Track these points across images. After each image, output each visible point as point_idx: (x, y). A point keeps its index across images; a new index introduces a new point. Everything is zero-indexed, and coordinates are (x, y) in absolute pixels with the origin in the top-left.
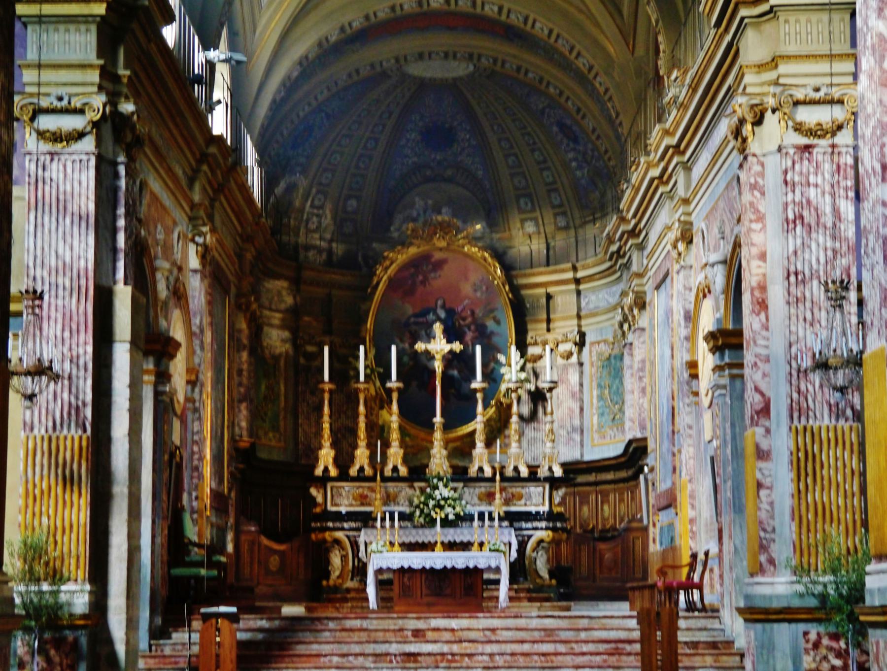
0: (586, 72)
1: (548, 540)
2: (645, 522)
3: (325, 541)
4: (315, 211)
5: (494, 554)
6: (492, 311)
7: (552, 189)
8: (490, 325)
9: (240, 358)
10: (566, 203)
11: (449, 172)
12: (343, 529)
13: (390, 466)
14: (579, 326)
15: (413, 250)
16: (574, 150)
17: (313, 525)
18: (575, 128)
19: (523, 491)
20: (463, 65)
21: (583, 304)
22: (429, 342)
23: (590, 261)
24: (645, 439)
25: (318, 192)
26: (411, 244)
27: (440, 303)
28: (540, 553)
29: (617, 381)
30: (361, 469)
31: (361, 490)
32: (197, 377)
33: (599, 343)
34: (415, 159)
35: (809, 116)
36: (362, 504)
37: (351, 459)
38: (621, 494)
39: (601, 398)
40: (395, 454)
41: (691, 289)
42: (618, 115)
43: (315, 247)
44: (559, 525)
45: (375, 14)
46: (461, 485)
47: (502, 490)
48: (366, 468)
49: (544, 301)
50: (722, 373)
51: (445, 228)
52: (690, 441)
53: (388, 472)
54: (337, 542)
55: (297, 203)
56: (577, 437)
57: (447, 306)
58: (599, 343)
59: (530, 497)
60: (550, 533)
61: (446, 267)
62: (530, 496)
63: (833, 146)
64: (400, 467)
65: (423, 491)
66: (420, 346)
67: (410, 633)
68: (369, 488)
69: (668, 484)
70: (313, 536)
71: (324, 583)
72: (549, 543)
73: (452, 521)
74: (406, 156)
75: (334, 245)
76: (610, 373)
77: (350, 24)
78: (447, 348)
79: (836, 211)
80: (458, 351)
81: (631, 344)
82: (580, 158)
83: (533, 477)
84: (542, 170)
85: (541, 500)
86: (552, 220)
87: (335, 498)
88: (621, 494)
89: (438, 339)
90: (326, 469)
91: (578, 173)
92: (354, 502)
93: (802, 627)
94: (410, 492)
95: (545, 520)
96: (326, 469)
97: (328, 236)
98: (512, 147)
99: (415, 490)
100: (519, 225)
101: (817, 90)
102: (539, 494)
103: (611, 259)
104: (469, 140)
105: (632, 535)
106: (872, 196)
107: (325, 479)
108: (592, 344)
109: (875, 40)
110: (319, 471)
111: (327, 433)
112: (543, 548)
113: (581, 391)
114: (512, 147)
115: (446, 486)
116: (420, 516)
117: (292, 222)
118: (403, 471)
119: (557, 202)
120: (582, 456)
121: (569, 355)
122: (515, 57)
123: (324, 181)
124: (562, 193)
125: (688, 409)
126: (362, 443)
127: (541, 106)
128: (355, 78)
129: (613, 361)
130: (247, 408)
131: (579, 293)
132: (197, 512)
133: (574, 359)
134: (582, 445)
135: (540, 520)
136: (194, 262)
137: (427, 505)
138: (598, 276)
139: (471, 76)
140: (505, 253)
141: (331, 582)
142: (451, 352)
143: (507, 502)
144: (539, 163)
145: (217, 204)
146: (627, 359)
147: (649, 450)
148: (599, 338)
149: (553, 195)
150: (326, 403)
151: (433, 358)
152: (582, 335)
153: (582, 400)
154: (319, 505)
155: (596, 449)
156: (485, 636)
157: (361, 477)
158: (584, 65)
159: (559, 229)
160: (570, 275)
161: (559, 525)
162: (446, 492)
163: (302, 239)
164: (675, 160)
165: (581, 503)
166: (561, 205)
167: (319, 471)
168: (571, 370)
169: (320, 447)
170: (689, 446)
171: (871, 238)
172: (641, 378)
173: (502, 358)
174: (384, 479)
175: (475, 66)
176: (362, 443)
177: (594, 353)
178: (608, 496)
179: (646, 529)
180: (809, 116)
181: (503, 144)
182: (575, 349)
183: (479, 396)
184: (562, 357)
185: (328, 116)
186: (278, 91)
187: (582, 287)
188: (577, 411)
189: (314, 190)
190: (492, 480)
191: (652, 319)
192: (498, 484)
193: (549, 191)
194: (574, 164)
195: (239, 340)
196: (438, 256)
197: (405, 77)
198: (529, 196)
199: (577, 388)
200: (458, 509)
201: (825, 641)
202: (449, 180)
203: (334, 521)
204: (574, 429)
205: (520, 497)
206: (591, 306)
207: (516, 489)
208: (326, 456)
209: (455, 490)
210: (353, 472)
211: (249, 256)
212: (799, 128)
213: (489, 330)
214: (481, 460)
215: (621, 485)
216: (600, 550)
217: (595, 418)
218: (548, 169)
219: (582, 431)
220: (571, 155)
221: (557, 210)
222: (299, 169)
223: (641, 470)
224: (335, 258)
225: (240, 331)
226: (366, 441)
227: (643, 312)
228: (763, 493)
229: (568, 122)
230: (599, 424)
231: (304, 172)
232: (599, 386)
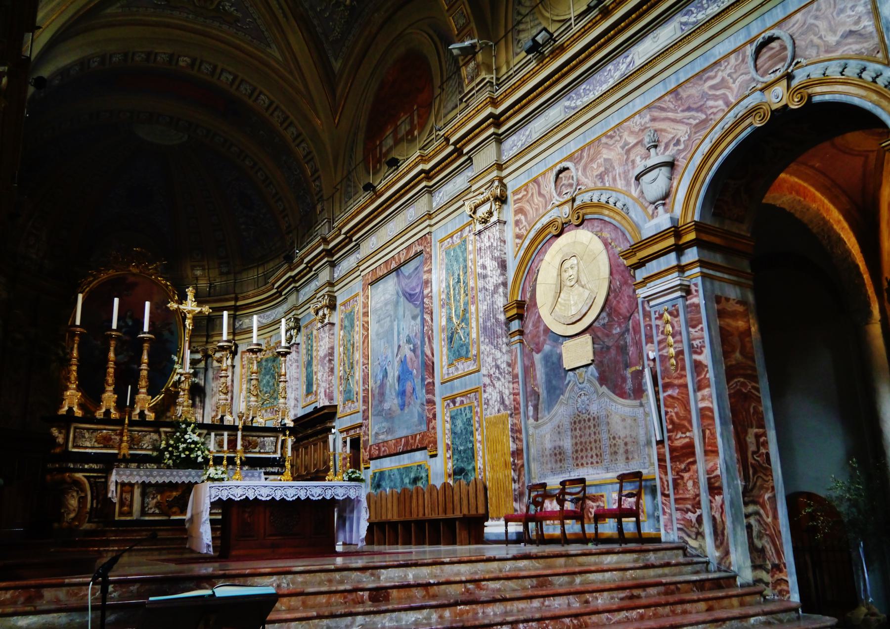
5: (353, 483)
8: (166, 334)
12: (83, 470)
13: (138, 411)
17: (49, 466)
19: (259, 440)
21: (237, 325)
29: (268, 377)
30: (108, 412)
37: (98, 401)
41: (505, 242)
42: (316, 171)
48: (112, 411)
50: (681, 275)
54: (77, 483)
59: (264, 446)
62: (264, 445)
65: (169, 436)
66: (173, 306)
67: (366, 594)
70: (48, 477)
71: (56, 525)
73: (201, 463)
78: (198, 309)
81: (298, 344)
87: (77, 439)
89: (189, 302)
94: (155, 436)
99: (160, 436)
102: (272, 443)
115: (193, 431)
116: (169, 459)
129: (264, 363)
137: (177, 448)
141: (65, 524)
142: (200, 312)
147: (338, 415)
154: (59, 445)
156: (468, 590)
160: (232, 303)
162: (195, 438)
164: (491, 130)
169: (67, 388)
172: (330, 360)
174: (132, 423)
177: (245, 359)
187: (238, 313)
194: (243, 227)
203: (74, 463)
206: (244, 327)
208: (72, 398)
209: (199, 435)
210: (99, 414)
223: (329, 430)
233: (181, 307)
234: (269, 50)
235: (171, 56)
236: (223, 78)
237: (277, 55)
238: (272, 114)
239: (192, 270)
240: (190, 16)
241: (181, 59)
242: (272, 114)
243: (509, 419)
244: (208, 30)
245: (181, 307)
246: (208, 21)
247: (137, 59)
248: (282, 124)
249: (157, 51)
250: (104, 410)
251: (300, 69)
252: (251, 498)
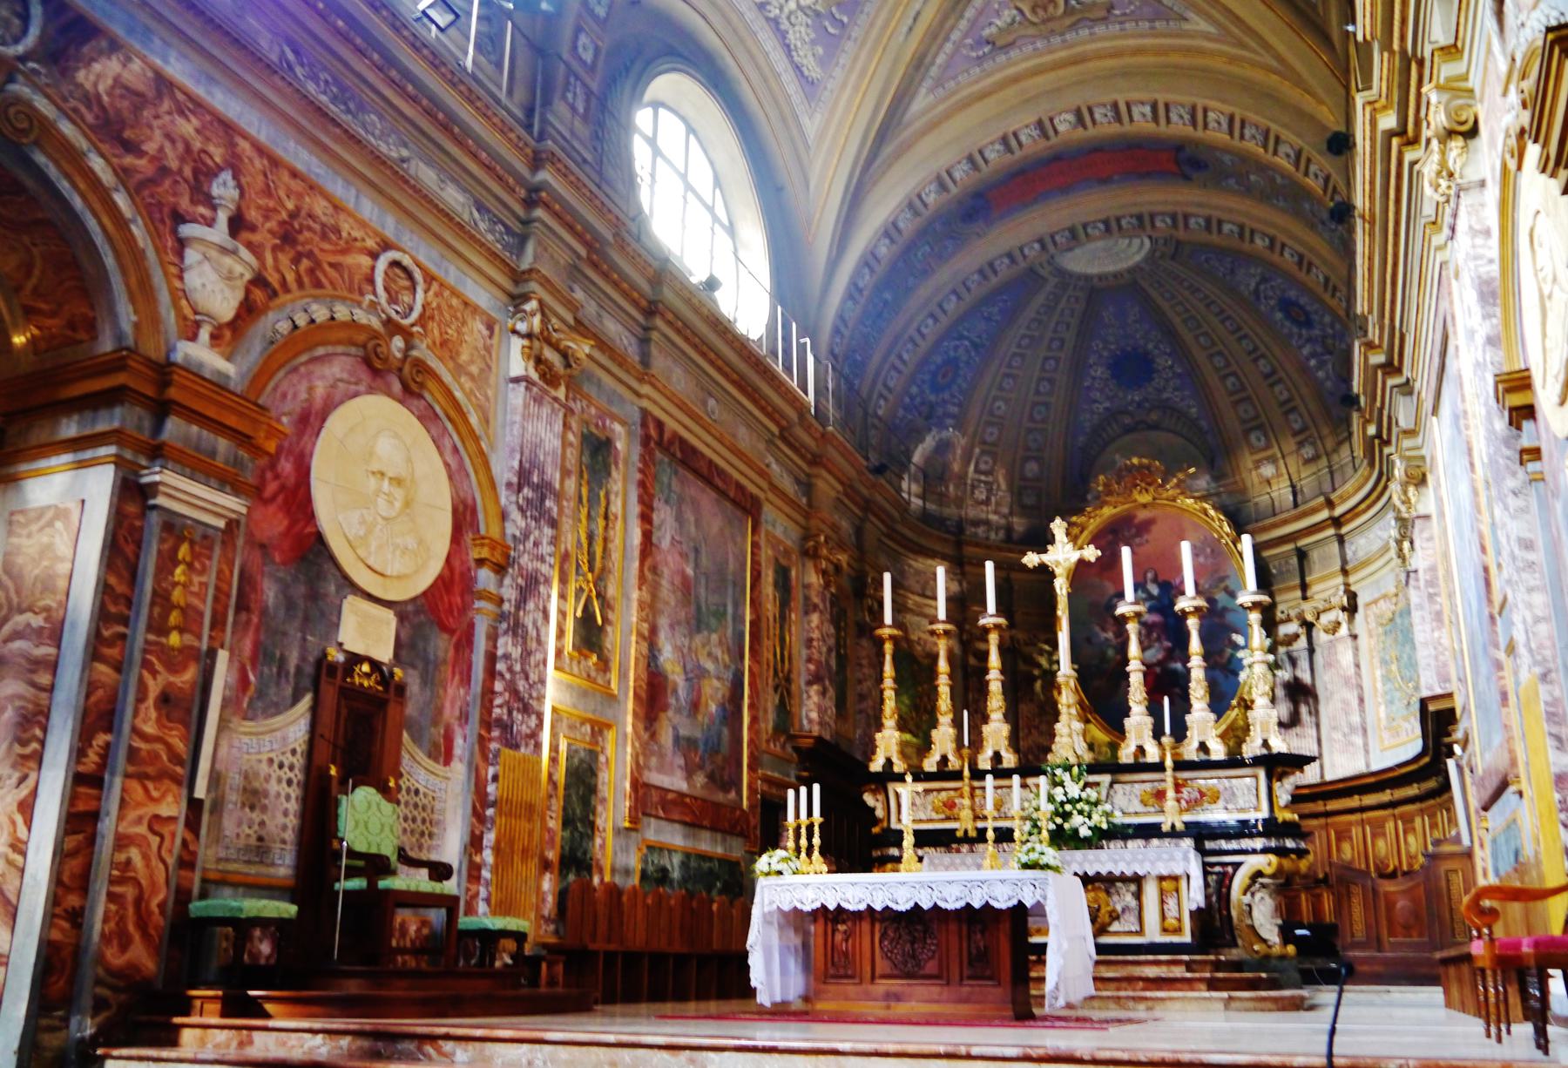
0: (1291, 168)
1: (1269, 871)
2: (1466, 841)
4: (983, 478)
5: (1030, 873)
6: (1222, 579)
7: (1288, 408)
9: (809, 622)
10: (1310, 424)
11: (1154, 416)
13: (989, 753)
14: (1347, 585)
15: (1107, 511)
16: (1309, 340)
18: (1303, 301)
20: (1136, 242)
22: (1045, 551)
23: (1349, 487)
24: (1450, 695)
25: (983, 452)
26: (1104, 503)
27: (1150, 575)
28: (1258, 896)
29: (1408, 648)
31: (944, 794)
32: (507, 556)
33: (1375, 602)
34: (1107, 404)
36: (948, 819)
38: (1432, 816)
39: (1387, 678)
40: (996, 732)
43: (987, 523)
44: (1290, 844)
45: (981, 152)
46: (1105, 779)
47: (1178, 787)
48: (951, 757)
49: (1294, 561)
51: (1143, 476)
52: (1532, 579)
53: (984, 763)
55: (956, 467)
56: (1358, 740)
57: (1160, 579)
58: (1375, 602)
60: (1273, 858)
61: (1155, 529)
62: (1233, 794)
64: (1003, 753)
66: (1031, 559)
68: (955, 789)
72: (1273, 876)
73: (1086, 839)
74: (1095, 401)
75: (1015, 520)
76: (1396, 640)
77: (949, 173)
78: (1075, 556)
80: (1093, 560)
82: (1319, 349)
83: (1234, 761)
84: (1272, 385)
85: (1254, 799)
86: (1294, 447)
88: (1432, 816)
89: (1058, 544)
90: (889, 762)
91: (1321, 374)
92: (934, 816)
95: (1260, 835)
96: (889, 762)
97: (1005, 510)
98: (1228, 365)
100: (1250, 465)
103: (1372, 464)
104: (1171, 367)
105: (1445, 866)
107: (889, 776)
108: (1367, 605)
110: (877, 765)
111: (890, 705)
112: (1263, 886)
113: (1358, 675)
114: (1228, 365)
115: (1076, 780)
117: (951, 488)
118: (1009, 760)
119: (1297, 426)
120: (1368, 765)
122: (1200, 205)
123: (989, 439)
124: (1302, 409)
125: (1513, 502)
126: (945, 720)
127: (1253, 285)
128: (994, 280)
129: (1398, 620)
130: (823, 693)
131: (1341, 540)
132: (494, 804)
133: (1344, 630)
134: (1367, 751)
135: (1251, 836)
136: (517, 362)
138: (1363, 506)
139: (1151, 258)
140: (1238, 510)
143: (1193, 804)
144: (1267, 376)
145: (655, 335)
146: (1414, 596)
148: (1377, 595)
149: (1292, 417)
150: (888, 658)
151: (1052, 575)
152: (1352, 597)
153: (1360, 687)
155: (1388, 753)
157: (944, 773)
158: (1288, 156)
159: (1307, 462)
160: (1324, 514)
161: (1290, 844)
162: (1074, 790)
165: (1374, 836)
166: (1304, 429)
167: (877, 765)
168: (1340, 648)
170: (1530, 590)
172: (1431, 597)
173: (1239, 639)
175: (1150, 237)
176: (945, 720)
178: (1412, 821)
179: (1469, 854)
181: (1202, 339)
182: (1343, 617)
184: (1326, 631)
185: (975, 346)
186: (857, 273)
187: (1344, 530)
188: (1355, 702)
189: (977, 451)
190: (1159, 767)
191: (1439, 500)
192: (1169, 772)
193: (1286, 413)
194: (1313, 362)
195: (807, 598)
196: (1142, 515)
197: (1061, 273)
198: (1260, 427)
199: (1352, 671)
200: (1096, 817)
202: (1155, 427)
204: (1352, 729)
205: (1215, 798)
207: (1205, 781)
211: (827, 487)
213: (1220, 605)
214: (1140, 736)
215: (1432, 802)
216: (1387, 894)
217: (1383, 708)
218: (1280, 381)
219: (1365, 730)
220: (1306, 351)
221: (1299, 438)
222: (949, 421)
224: (1015, 536)
225: (807, 586)
226: (951, 716)
227: (1423, 490)
229: (1292, 294)
230: (1388, 717)
231: (960, 426)
232: (1384, 662)
233: (1046, 558)
234: (1186, 26)
235: (1040, 124)
236: (1136, 116)
237: (1203, 25)
238: (1242, 137)
239: (1257, 467)
240: (1039, 45)
241: (1056, 121)
242: (1242, 137)
243: (1543, 689)
244: (1079, 49)
245: (1046, 558)
246: (1068, 37)
247: (991, 155)
248: (1265, 146)
249: (1011, 129)
250: (937, 757)
251: (1250, 31)
252: (926, 905)
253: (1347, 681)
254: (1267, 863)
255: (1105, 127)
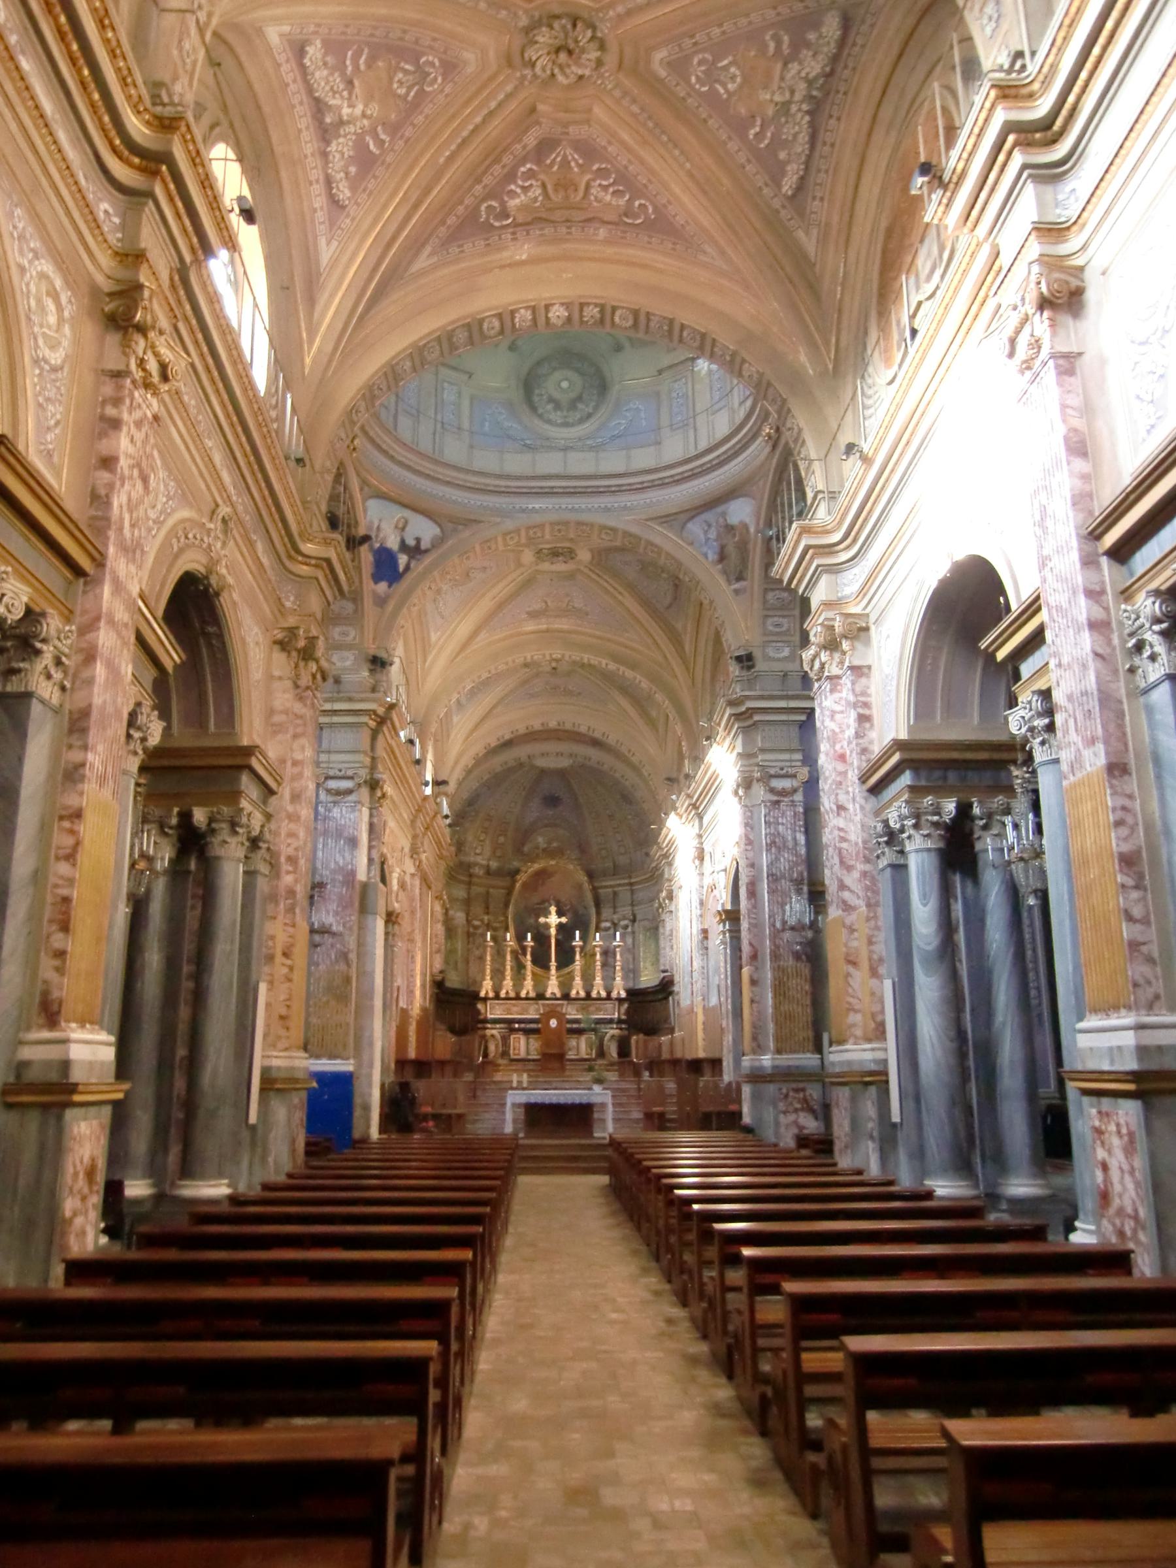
3: (484, 1036)
15: (537, 866)
35: (779, 784)
53: (523, 994)
54: (493, 1036)
63: (793, 801)
66: (542, 920)
69: (689, 1002)
78: (559, 920)
79: (795, 839)
93: (777, 1086)
101: (782, 769)
106: (831, 825)
107: (485, 999)
109: (830, 734)
111: (488, 971)
121: (626, 927)
131: (632, 892)
133: (629, 929)
146: (661, 930)
152: (634, 916)
160: (626, 881)
163: (472, 859)
167: (482, 994)
169: (484, 979)
171: (830, 849)
180: (779, 784)
183: (578, 950)
197: (533, 767)
201: (791, 1094)
212: (772, 791)
228: (755, 1005)
253: (629, 950)
254: (616, 1032)
255: (568, 726)
